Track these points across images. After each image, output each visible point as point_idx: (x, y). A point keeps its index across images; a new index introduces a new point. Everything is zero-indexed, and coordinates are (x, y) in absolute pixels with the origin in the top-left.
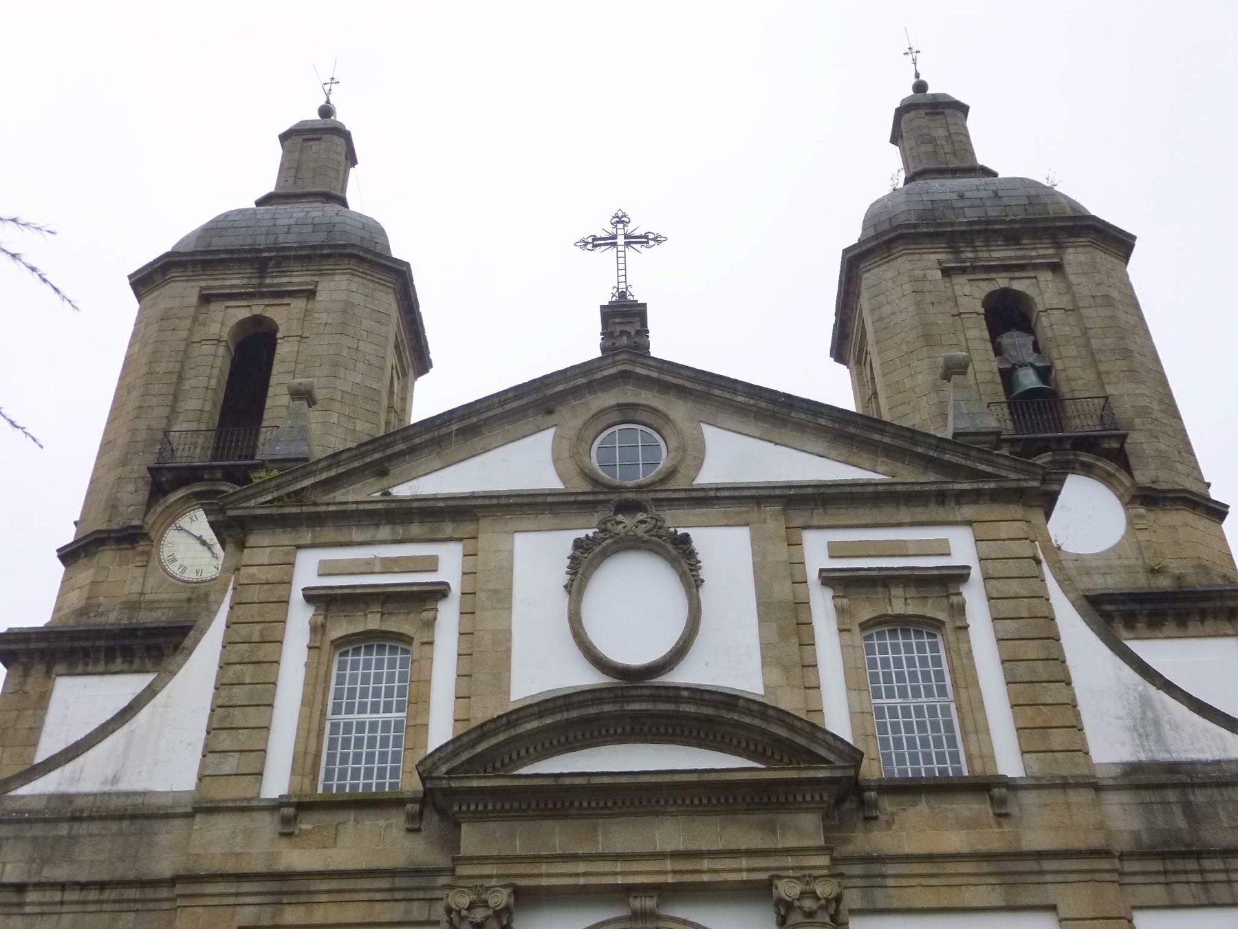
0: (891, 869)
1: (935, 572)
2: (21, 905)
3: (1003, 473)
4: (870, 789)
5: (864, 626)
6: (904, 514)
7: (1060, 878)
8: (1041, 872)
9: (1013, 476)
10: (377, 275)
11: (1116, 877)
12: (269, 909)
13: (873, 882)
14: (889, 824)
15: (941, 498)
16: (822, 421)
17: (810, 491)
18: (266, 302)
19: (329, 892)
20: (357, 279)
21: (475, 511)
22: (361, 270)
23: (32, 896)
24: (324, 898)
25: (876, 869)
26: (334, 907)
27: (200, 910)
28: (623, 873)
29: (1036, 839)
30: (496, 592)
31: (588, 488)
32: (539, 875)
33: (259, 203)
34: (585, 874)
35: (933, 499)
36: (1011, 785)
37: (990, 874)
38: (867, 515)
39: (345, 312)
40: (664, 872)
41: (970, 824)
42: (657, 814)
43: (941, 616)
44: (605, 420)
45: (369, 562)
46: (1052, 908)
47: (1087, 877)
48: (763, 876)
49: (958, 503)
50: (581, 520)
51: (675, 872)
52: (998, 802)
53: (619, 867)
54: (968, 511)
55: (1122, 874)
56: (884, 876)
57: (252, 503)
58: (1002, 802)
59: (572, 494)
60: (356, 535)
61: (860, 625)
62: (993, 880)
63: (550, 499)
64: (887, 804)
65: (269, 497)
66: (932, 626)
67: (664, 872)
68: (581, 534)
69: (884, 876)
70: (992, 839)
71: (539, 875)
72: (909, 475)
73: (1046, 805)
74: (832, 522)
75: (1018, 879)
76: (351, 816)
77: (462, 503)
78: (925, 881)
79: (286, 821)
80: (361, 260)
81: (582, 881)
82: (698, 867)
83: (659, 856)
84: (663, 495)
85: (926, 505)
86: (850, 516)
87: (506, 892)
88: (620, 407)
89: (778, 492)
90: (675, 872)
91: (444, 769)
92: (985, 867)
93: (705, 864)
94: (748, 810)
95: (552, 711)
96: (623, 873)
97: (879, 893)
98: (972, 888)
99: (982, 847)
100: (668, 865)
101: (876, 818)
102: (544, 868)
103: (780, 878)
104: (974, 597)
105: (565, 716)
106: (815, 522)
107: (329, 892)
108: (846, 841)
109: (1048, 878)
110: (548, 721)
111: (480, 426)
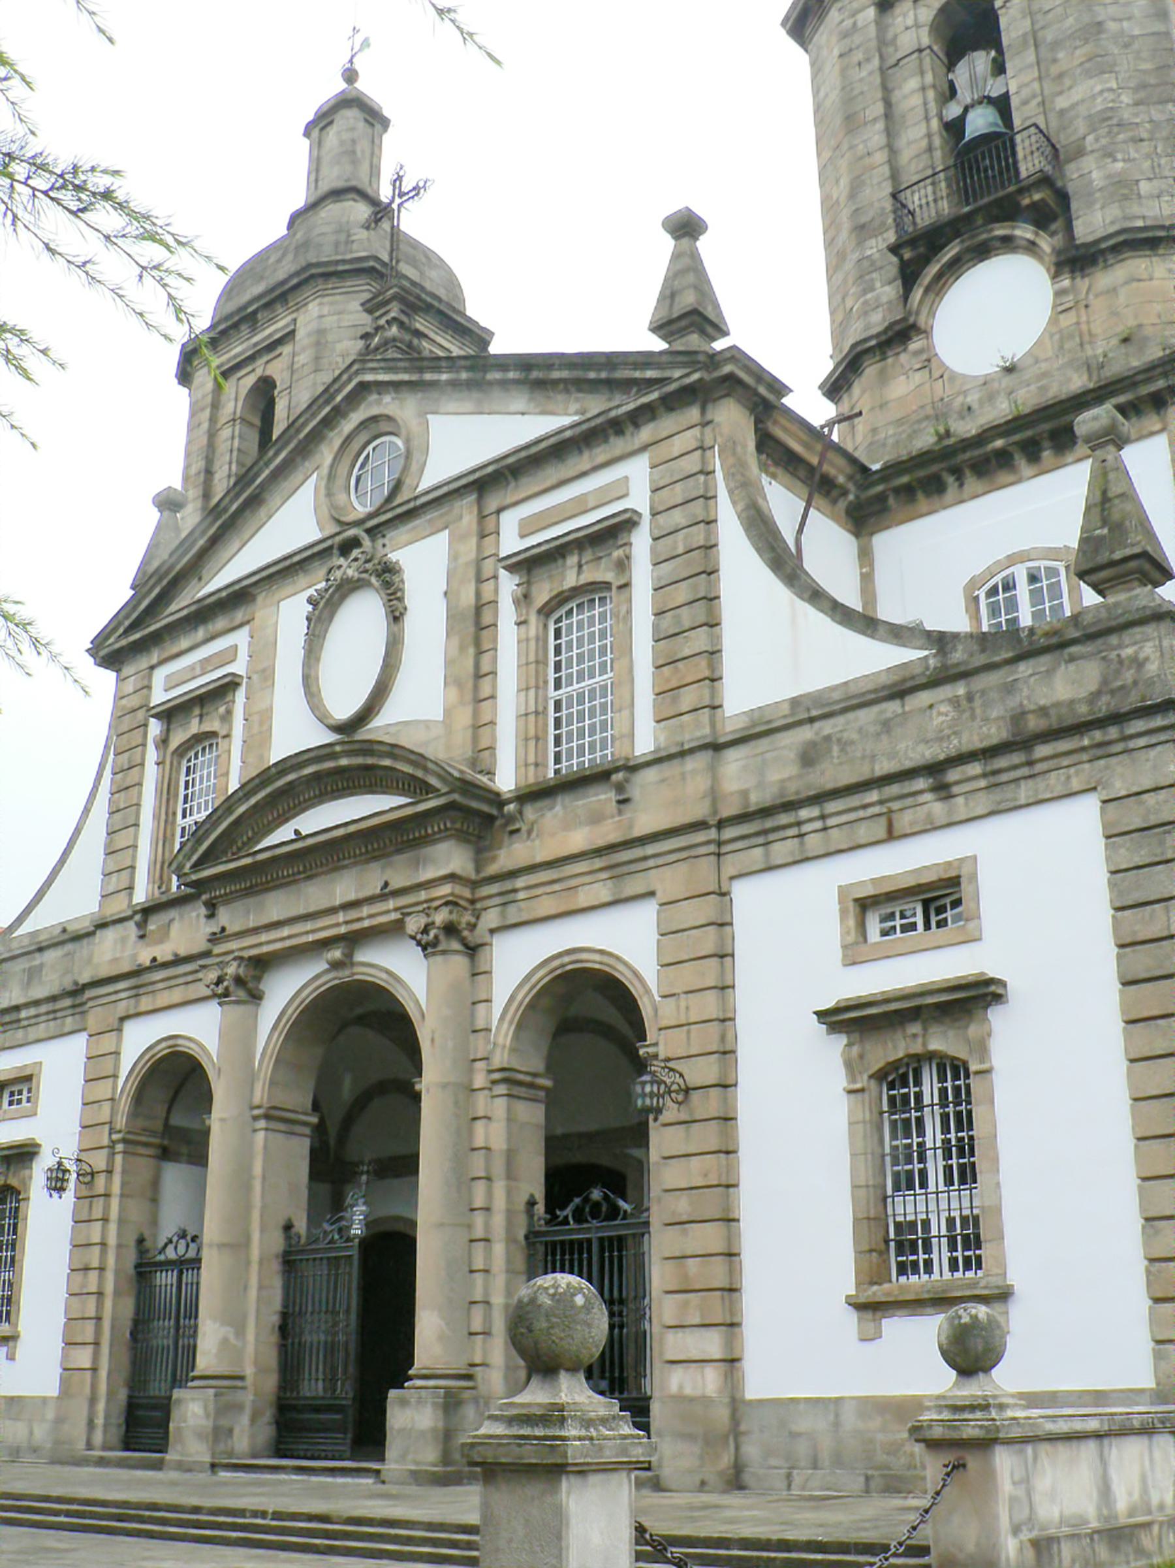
0: (520, 882)
1: (596, 528)
2: (19, 1021)
3: (667, 374)
4: (509, 801)
5: (546, 611)
6: (584, 461)
7: (660, 861)
8: (645, 858)
9: (677, 374)
10: (348, 284)
11: (712, 848)
12: (132, 1001)
13: (508, 899)
14: (529, 832)
15: (616, 426)
16: (511, 375)
17: (490, 469)
18: (265, 358)
19: (162, 980)
20: (326, 299)
21: (250, 590)
22: (330, 286)
23: (23, 1014)
24: (161, 986)
25: (507, 885)
26: (166, 993)
27: (99, 1009)
28: (313, 931)
29: (646, 821)
30: (264, 670)
31: (338, 529)
32: (261, 944)
33: (288, 229)
34: (289, 937)
35: (611, 431)
36: (633, 768)
37: (602, 869)
38: (552, 473)
39: (318, 343)
40: (338, 925)
41: (596, 819)
42: (336, 869)
43: (609, 576)
44: (356, 445)
45: (192, 668)
46: (652, 894)
47: (684, 855)
48: (394, 916)
49: (637, 426)
50: (302, 580)
51: (347, 923)
52: (620, 788)
53: (309, 926)
54: (646, 433)
55: (720, 844)
56: (515, 891)
57: (111, 640)
58: (620, 788)
59: (328, 538)
60: (184, 643)
61: (539, 611)
62: (604, 875)
63: (296, 559)
64: (530, 812)
65: (121, 630)
66: (601, 590)
67: (338, 925)
68: (311, 591)
69: (515, 891)
70: (609, 833)
71: (261, 944)
72: (596, 405)
73: (663, 781)
74: (523, 495)
75: (625, 869)
76: (173, 913)
77: (237, 587)
78: (548, 889)
79: (142, 925)
80: (327, 276)
81: (288, 943)
82: (359, 915)
83: (333, 911)
84: (399, 511)
85: (606, 440)
86: (529, 485)
87: (235, 964)
88: (364, 424)
89: (464, 482)
90: (347, 923)
91: (188, 865)
92: (598, 863)
93: (365, 911)
94: (399, 851)
95: (254, 792)
96: (313, 931)
97: (512, 909)
98: (587, 887)
99: (601, 843)
100: (341, 917)
101: (518, 831)
102: (264, 937)
103: (409, 914)
104: (641, 543)
105: (269, 790)
106: (509, 501)
107: (162, 980)
108: (494, 859)
109: (651, 863)
110: (253, 801)
111: (259, 494)
